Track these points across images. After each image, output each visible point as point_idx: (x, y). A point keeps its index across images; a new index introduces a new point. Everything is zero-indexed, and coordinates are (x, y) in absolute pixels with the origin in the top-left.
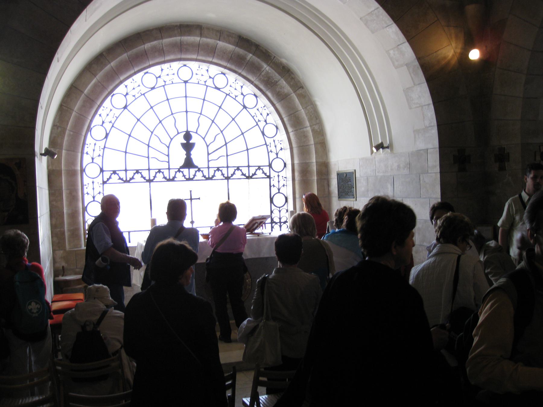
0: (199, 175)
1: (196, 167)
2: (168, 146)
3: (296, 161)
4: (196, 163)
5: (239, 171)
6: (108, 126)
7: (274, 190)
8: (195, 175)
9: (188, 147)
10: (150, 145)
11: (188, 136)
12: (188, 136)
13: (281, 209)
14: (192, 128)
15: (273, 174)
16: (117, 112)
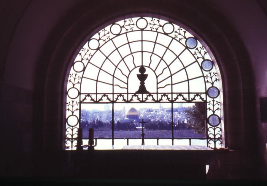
0: (150, 99)
2: (127, 76)
5: (181, 96)
8: (147, 99)
9: (142, 77)
10: (115, 76)
11: (142, 69)
12: (142, 69)
13: (215, 127)
14: (146, 63)
15: (209, 99)
16: (92, 52)
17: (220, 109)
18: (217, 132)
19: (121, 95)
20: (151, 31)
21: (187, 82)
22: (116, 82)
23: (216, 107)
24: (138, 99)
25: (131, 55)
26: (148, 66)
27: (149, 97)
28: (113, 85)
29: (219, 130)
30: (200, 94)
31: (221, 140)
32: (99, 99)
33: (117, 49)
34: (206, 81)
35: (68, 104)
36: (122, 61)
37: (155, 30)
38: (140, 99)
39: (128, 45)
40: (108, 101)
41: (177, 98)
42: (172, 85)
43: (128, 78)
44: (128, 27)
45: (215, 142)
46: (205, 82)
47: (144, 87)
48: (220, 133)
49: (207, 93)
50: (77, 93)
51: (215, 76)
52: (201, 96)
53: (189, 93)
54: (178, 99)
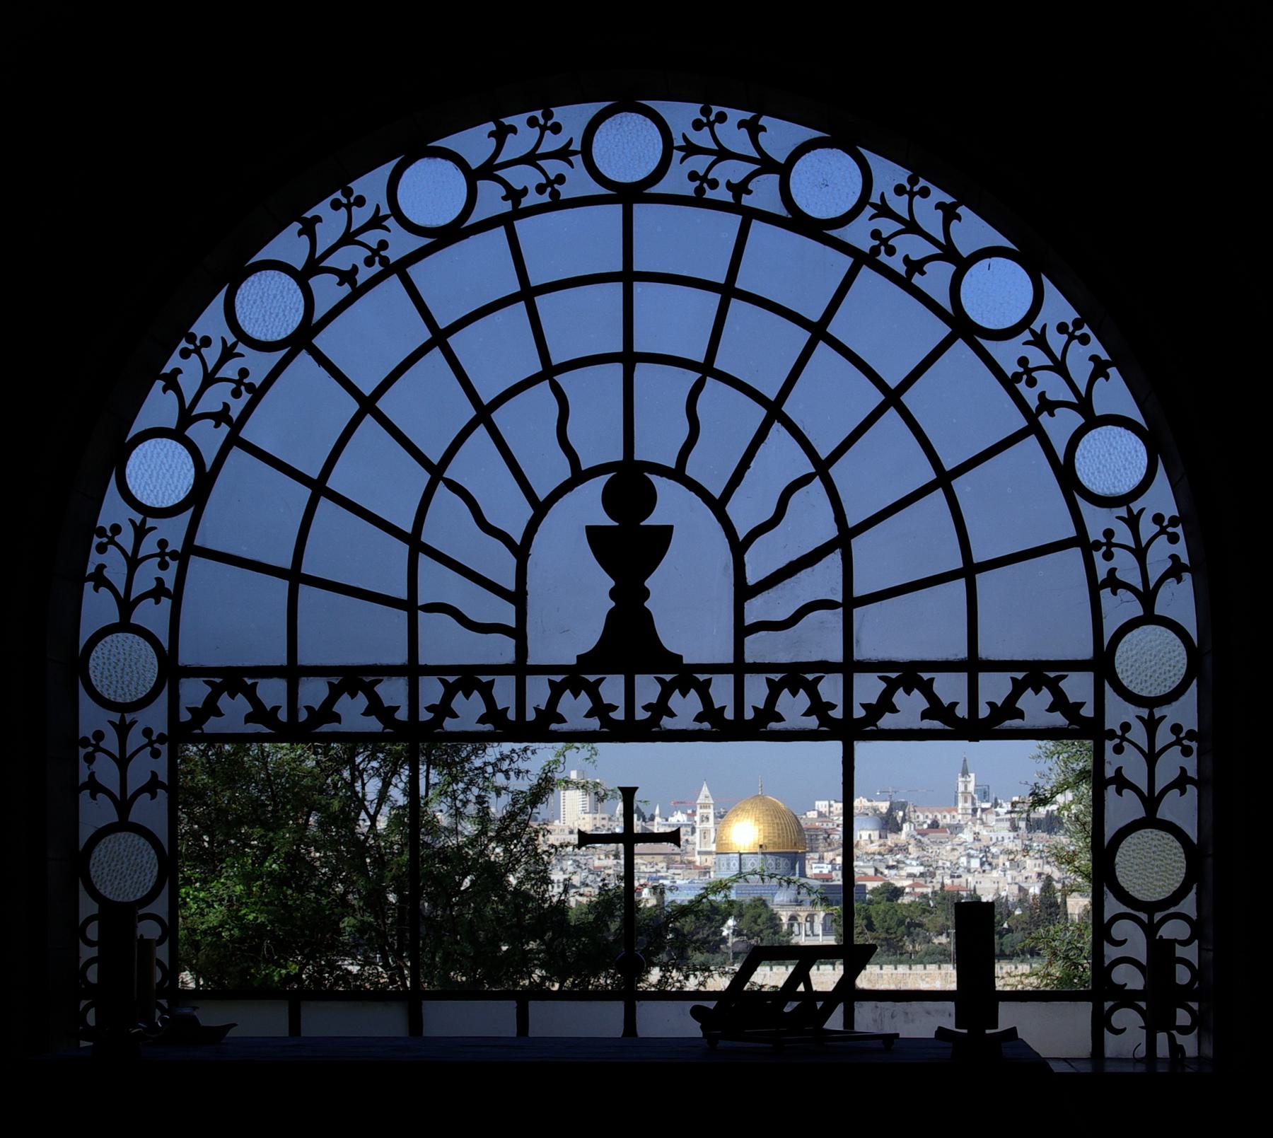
0: (686, 708)
4: (672, 636)
7: (1123, 807)
8: (660, 708)
13: (1158, 916)
15: (1118, 712)
20: (698, 200)
21: (960, 585)
24: (600, 709)
25: (545, 385)
26: (672, 464)
27: (675, 701)
28: (410, 605)
30: (1052, 675)
31: (1195, 1006)
32: (309, 708)
33: (440, 338)
34: (1102, 575)
36: (481, 431)
37: (727, 197)
38: (613, 708)
40: (373, 725)
41: (885, 704)
42: (850, 603)
43: (521, 552)
44: (523, 177)
46: (1095, 589)
47: (648, 615)
50: (147, 665)
51: (1164, 538)
54: (894, 710)
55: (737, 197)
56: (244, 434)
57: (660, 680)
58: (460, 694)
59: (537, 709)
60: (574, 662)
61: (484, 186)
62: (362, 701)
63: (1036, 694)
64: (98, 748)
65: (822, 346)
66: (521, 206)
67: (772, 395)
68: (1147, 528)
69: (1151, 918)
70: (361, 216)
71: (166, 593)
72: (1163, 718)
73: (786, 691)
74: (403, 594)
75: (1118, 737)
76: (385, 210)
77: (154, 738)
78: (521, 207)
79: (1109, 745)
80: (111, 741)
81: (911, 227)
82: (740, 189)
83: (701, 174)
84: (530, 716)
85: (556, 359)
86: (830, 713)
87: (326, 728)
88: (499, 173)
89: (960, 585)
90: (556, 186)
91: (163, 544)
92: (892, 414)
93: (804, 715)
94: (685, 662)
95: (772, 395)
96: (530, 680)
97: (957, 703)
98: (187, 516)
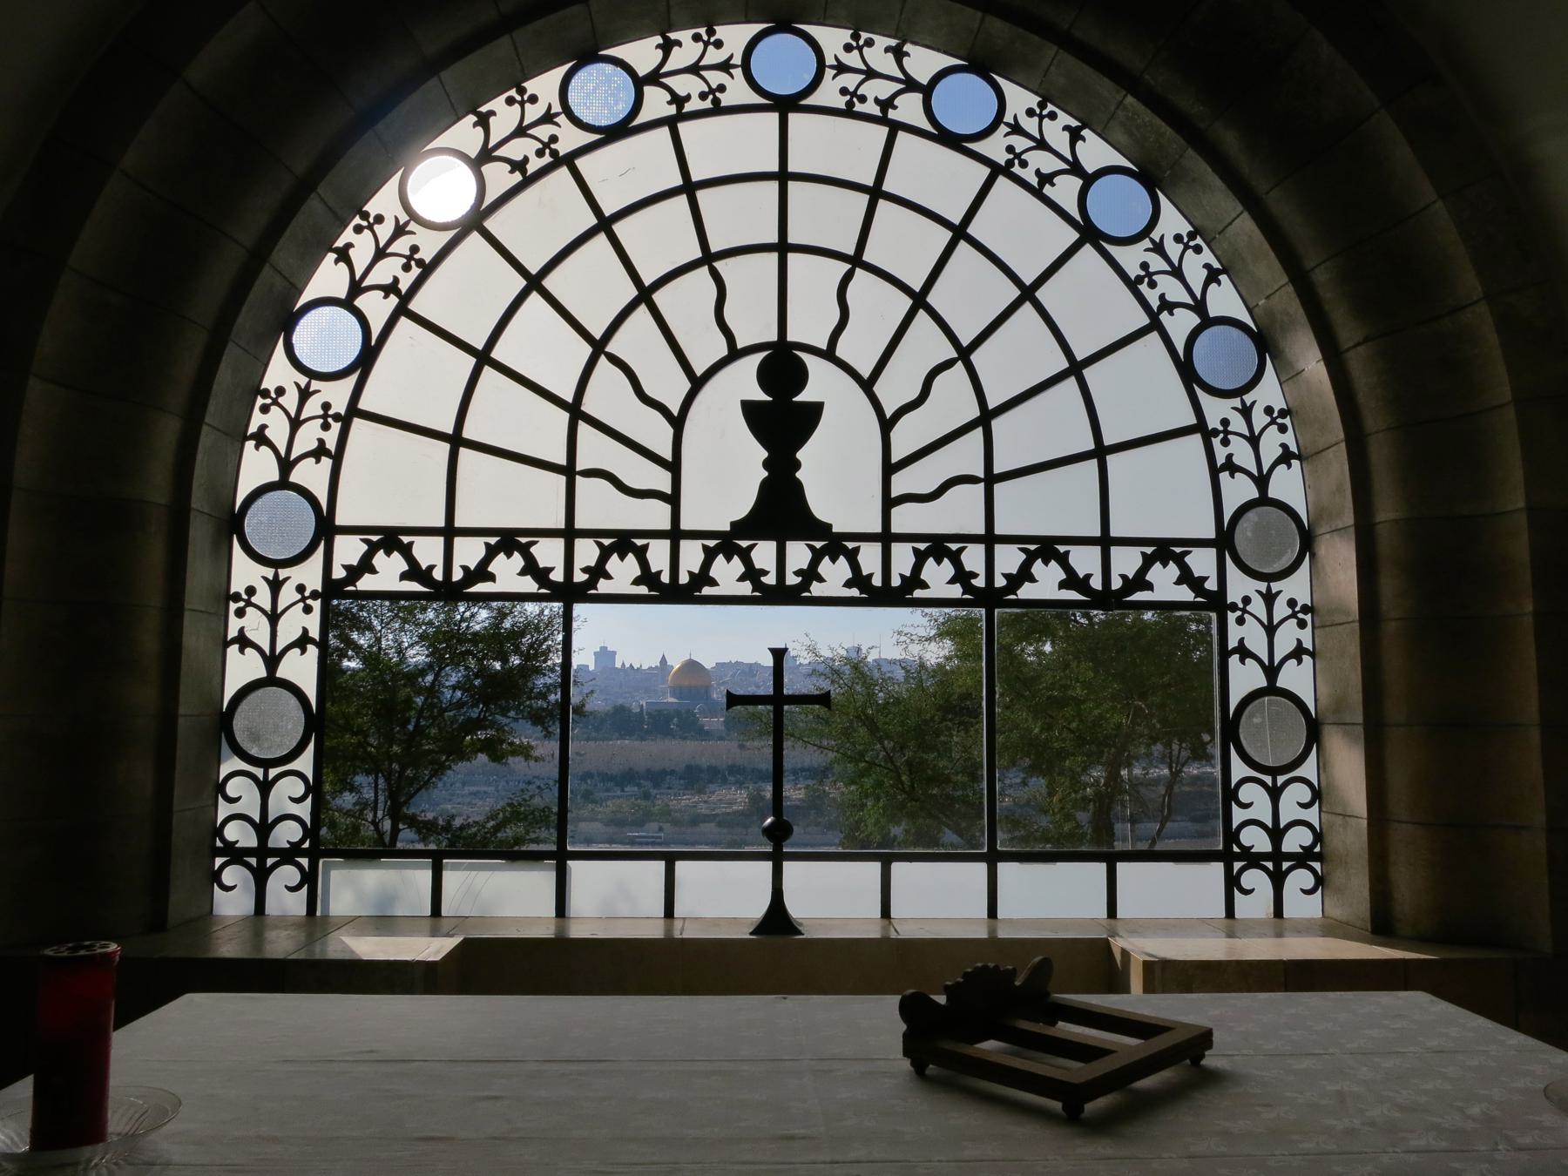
0: (835, 574)
1: (822, 530)
3: (1386, 512)
4: (821, 505)
5: (1053, 563)
6: (377, 307)
8: (810, 574)
13: (1281, 779)
14: (809, 327)
15: (1239, 586)
17: (1312, 654)
18: (1290, 808)
19: (623, 542)
20: (848, 113)
21: (1093, 464)
22: (594, 449)
23: (1288, 636)
24: (752, 574)
25: (706, 268)
26: (824, 347)
27: (825, 566)
28: (569, 471)
29: (1305, 794)
30: (1178, 550)
31: (1317, 866)
32: (465, 568)
34: (1221, 460)
35: (242, 604)
36: (642, 311)
37: (876, 111)
38: (765, 573)
39: (682, 201)
42: (991, 479)
43: (678, 423)
44: (686, 85)
45: (1278, 879)
47: (798, 487)
48: (1312, 815)
49: (1224, 541)
52: (1187, 559)
53: (1105, 541)
54: (1033, 580)
55: (884, 110)
56: (414, 306)
57: (811, 548)
58: (615, 557)
59: (690, 573)
60: (728, 528)
61: (650, 91)
62: (517, 561)
63: (1164, 567)
64: (249, 603)
65: (963, 246)
66: (684, 111)
67: (917, 288)
68: (1259, 419)
69: (1275, 781)
70: (534, 112)
71: (327, 453)
72: (1279, 593)
73: (931, 561)
74: (561, 460)
75: (1240, 609)
76: (557, 108)
77: (307, 594)
78: (684, 111)
79: (1232, 617)
80: (263, 597)
81: (1042, 144)
82: (887, 104)
83: (851, 89)
84: (684, 579)
85: (715, 247)
86: (974, 582)
87: (481, 588)
88: (664, 80)
89: (1093, 464)
90: (718, 94)
91: (326, 406)
92: (1027, 307)
93: (947, 583)
94: (834, 530)
95: (917, 288)
96: (685, 545)
97: (1091, 575)
98: (352, 380)
